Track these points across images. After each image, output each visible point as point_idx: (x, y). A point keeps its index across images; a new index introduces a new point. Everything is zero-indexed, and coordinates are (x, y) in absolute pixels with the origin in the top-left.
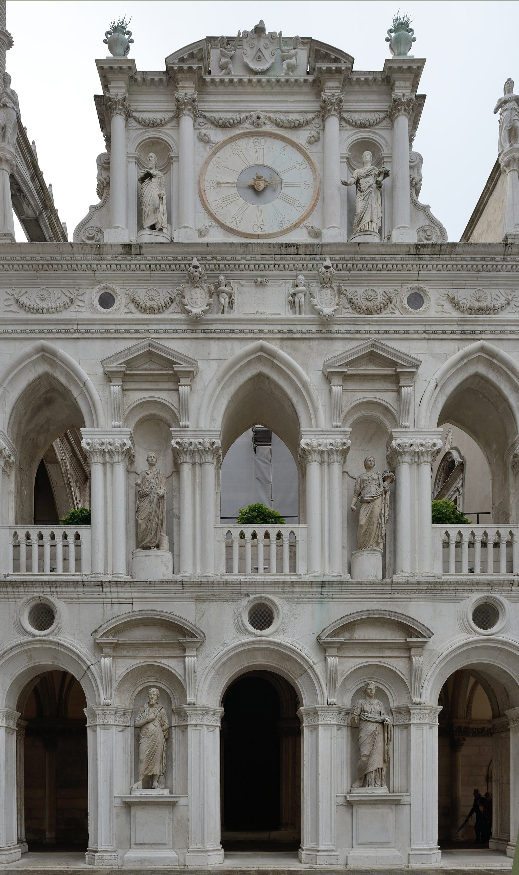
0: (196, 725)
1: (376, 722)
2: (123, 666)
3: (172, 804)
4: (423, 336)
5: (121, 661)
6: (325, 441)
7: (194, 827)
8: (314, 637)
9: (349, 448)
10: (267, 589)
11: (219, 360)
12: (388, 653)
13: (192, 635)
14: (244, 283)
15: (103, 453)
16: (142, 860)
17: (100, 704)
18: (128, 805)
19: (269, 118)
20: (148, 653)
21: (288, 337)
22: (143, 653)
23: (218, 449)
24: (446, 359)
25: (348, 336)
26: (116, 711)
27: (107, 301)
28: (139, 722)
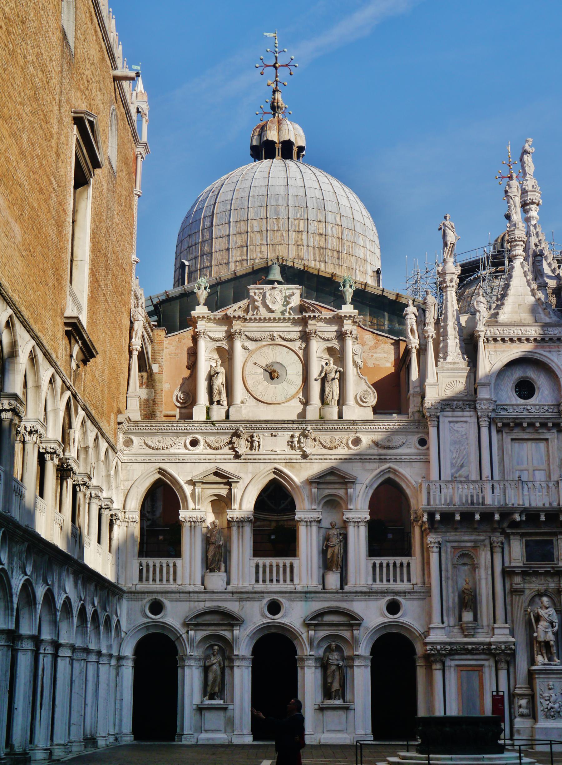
0: (238, 666)
1: (335, 665)
2: (200, 635)
3: (225, 709)
4: (359, 461)
5: (198, 632)
6: (308, 516)
7: (237, 721)
8: (302, 620)
9: (321, 520)
10: (277, 595)
12: (341, 628)
13: (238, 620)
14: (266, 434)
15: (190, 522)
16: (208, 739)
17: (187, 655)
18: (200, 709)
19: (281, 337)
20: (213, 628)
21: (289, 462)
22: (210, 628)
23: (251, 520)
24: (372, 472)
25: (321, 461)
26: (195, 658)
27: (194, 443)
28: (208, 664)
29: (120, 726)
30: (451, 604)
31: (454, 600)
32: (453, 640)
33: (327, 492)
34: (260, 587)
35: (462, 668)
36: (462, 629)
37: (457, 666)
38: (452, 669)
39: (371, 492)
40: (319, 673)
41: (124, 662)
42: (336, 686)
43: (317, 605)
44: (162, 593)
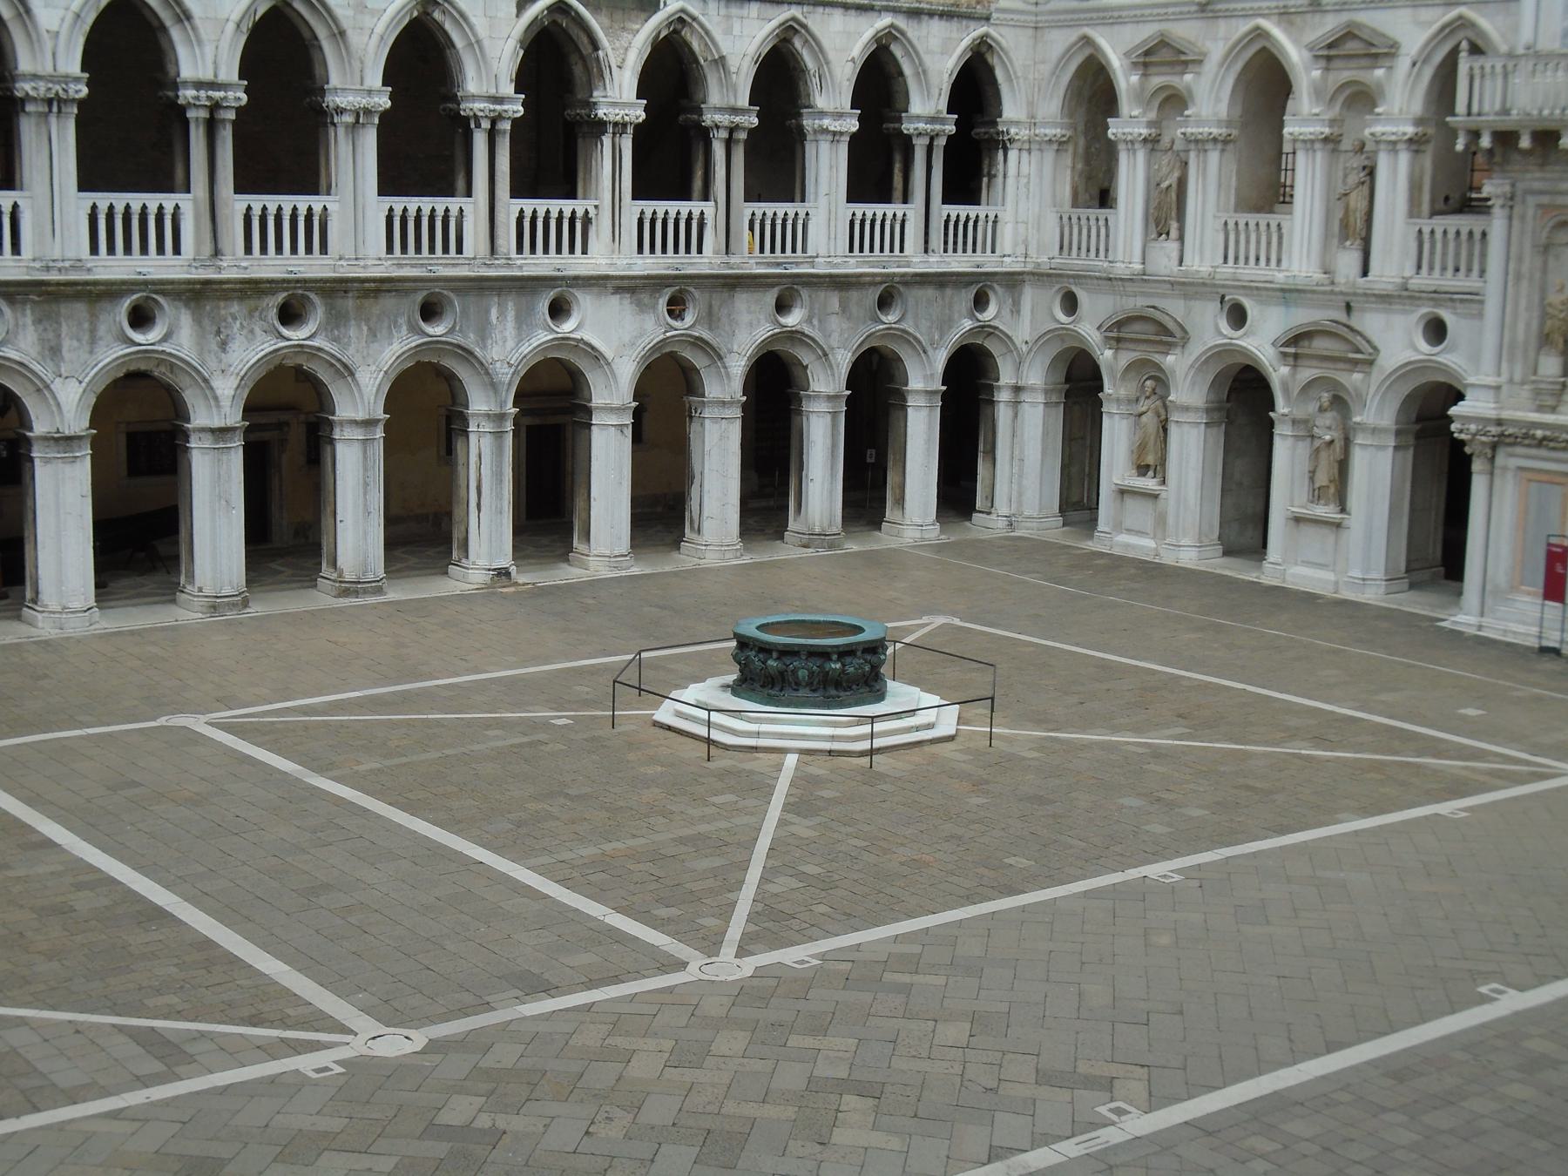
2: (1126, 358)
11: (1226, 39)
12: (1341, 365)
16: (1127, 546)
18: (1123, 492)
29: (1020, 503)
30: (1521, 336)
31: (1528, 325)
32: (1506, 414)
33: (1346, 75)
34: (1228, 270)
35: (1529, 475)
36: (1537, 393)
37: (1521, 469)
38: (1509, 475)
39: (1428, 73)
40: (1304, 449)
41: (1025, 397)
42: (1322, 479)
43: (1302, 317)
44: (1073, 277)
